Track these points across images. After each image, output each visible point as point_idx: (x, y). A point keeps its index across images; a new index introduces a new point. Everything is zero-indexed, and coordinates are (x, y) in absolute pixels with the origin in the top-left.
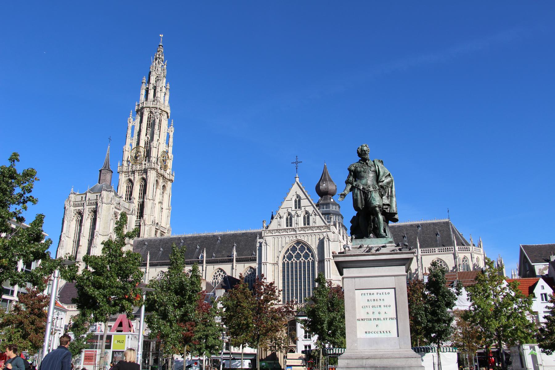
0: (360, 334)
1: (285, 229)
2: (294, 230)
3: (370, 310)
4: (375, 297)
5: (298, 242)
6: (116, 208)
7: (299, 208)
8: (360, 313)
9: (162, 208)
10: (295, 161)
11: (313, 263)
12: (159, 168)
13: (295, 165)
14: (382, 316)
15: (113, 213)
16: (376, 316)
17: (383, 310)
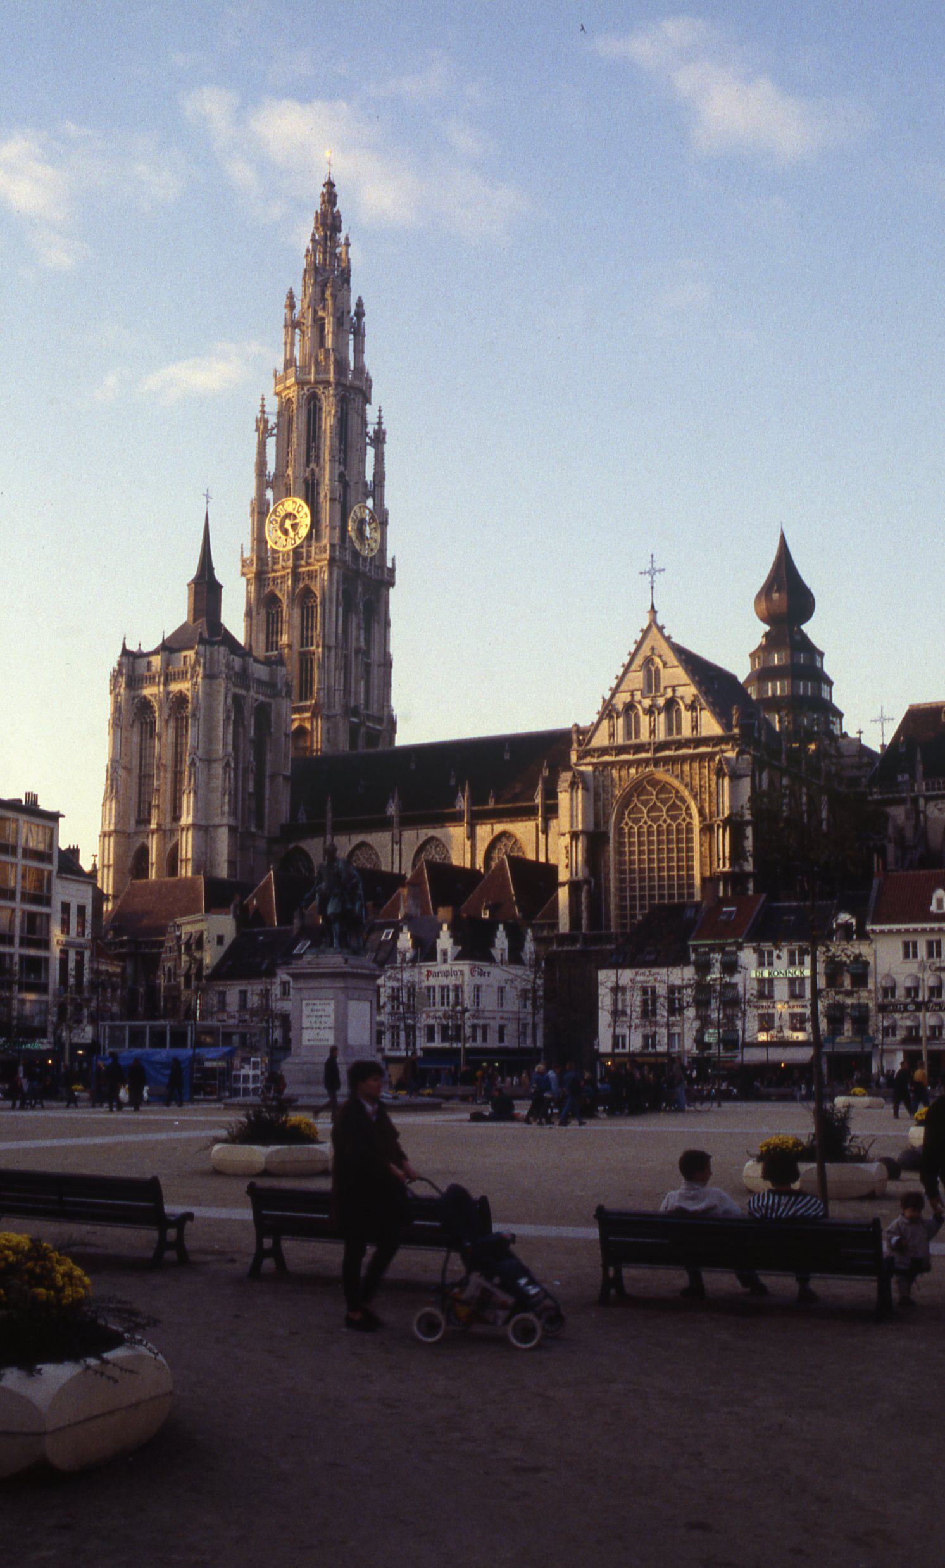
0: (305, 1042)
1: (621, 750)
2: (639, 748)
3: (314, 1019)
4: (318, 1007)
5: (654, 783)
6: (235, 685)
7: (657, 689)
8: (306, 1023)
9: (368, 665)
10: (648, 567)
11: (690, 830)
12: (348, 557)
13: (657, 566)
14: (322, 1026)
15: (229, 700)
16: (318, 1025)
17: (323, 1020)
